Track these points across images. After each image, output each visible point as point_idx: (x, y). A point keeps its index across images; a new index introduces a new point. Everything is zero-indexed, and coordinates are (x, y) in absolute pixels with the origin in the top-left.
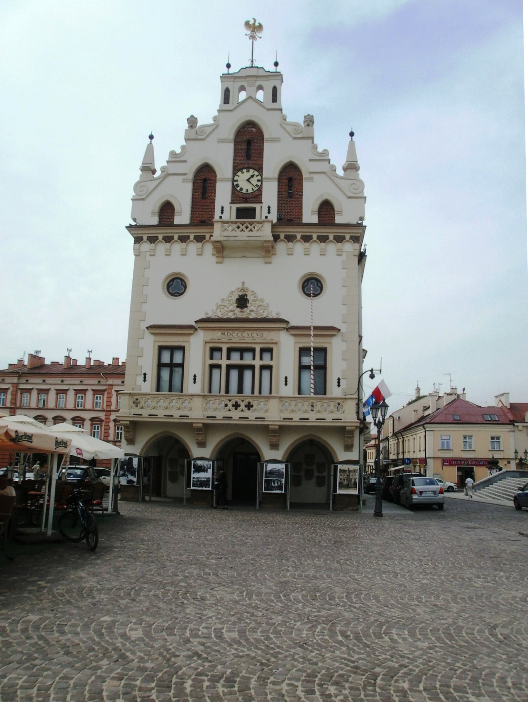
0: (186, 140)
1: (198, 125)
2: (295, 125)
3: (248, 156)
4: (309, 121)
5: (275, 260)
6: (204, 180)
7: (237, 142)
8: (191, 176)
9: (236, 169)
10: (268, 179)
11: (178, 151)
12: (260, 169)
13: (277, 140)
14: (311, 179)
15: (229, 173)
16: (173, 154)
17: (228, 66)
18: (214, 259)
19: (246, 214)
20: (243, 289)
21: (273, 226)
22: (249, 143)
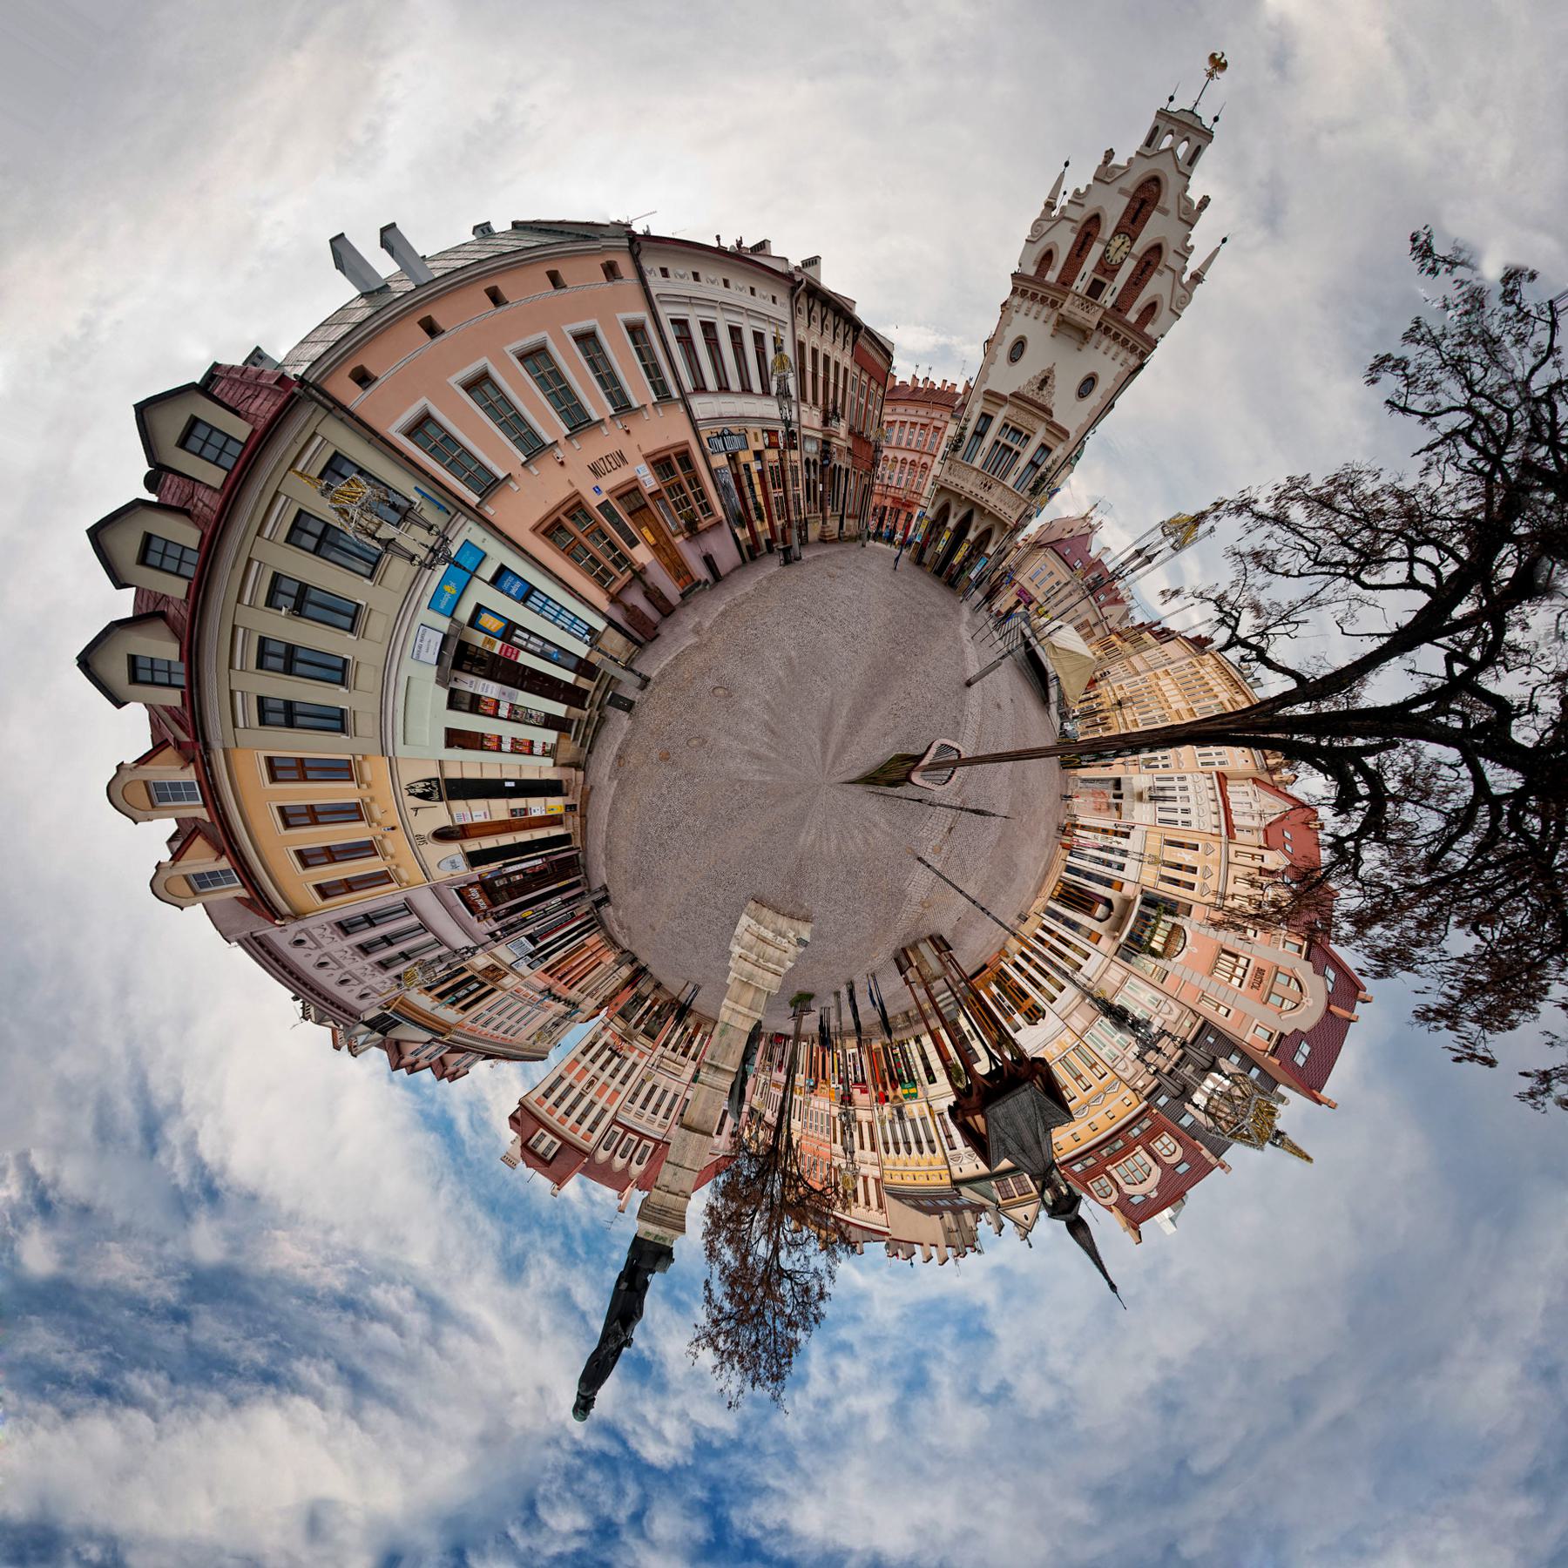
0: (1095, 178)
1: (1113, 162)
2: (1190, 202)
3: (1133, 221)
4: (1205, 201)
5: (1088, 349)
6: (1089, 231)
7: (1133, 199)
8: (1079, 226)
9: (1117, 232)
10: (1134, 256)
11: (1082, 190)
12: (1133, 240)
13: (1165, 212)
14: (1161, 273)
15: (1108, 236)
16: (1077, 191)
17: (1171, 99)
18: (1049, 329)
19: (1096, 289)
20: (1051, 371)
21: (1105, 313)
22: (1143, 202)
